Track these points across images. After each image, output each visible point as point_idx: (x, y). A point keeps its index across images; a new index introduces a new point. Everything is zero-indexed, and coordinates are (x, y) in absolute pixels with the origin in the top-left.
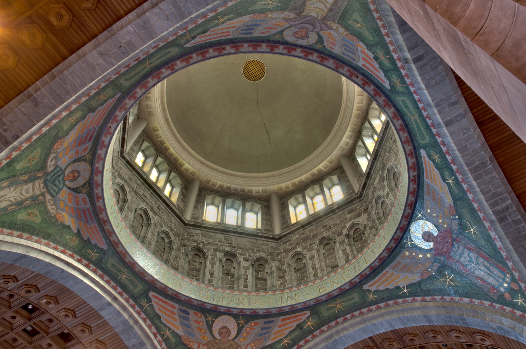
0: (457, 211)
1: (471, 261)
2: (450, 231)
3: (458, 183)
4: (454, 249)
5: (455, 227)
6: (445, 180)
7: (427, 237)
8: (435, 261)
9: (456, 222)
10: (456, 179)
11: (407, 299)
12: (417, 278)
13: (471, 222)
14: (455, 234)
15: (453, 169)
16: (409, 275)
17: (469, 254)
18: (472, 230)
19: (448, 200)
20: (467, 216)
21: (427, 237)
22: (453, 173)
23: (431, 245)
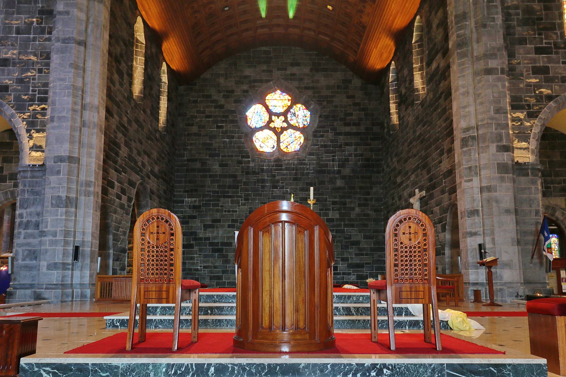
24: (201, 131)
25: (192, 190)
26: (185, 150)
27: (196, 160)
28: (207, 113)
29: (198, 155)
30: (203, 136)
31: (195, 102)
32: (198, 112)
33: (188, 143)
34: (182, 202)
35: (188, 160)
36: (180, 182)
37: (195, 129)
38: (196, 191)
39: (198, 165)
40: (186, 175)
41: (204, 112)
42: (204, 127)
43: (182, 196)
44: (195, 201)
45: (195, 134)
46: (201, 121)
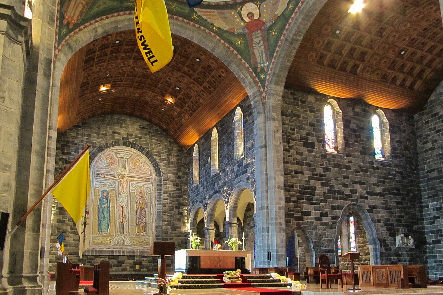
0: (277, 20)
1: (259, 44)
2: (264, 23)
3: (293, 10)
4: (256, 32)
5: (268, 24)
6: (289, 3)
7: (250, 15)
8: (242, 29)
9: (271, 23)
10: (294, 9)
11: (212, 33)
12: (226, 28)
13: (277, 30)
14: (264, 27)
15: (298, 4)
16: (224, 24)
17: (260, 40)
18: (274, 33)
19: (279, 12)
20: (278, 26)
21: (250, 15)
22: (296, 5)
23: (247, 20)
24: (434, 145)
25: (434, 196)
26: (425, 164)
27: (433, 170)
28: (437, 129)
29: (434, 165)
30: (436, 148)
31: (427, 123)
32: (431, 130)
33: (426, 158)
34: (428, 206)
35: (428, 172)
36: (425, 190)
37: (429, 145)
38: (437, 195)
39: (435, 174)
40: (428, 184)
41: (434, 129)
42: (436, 141)
43: (427, 202)
44: (437, 204)
45: (430, 149)
46: (433, 137)
